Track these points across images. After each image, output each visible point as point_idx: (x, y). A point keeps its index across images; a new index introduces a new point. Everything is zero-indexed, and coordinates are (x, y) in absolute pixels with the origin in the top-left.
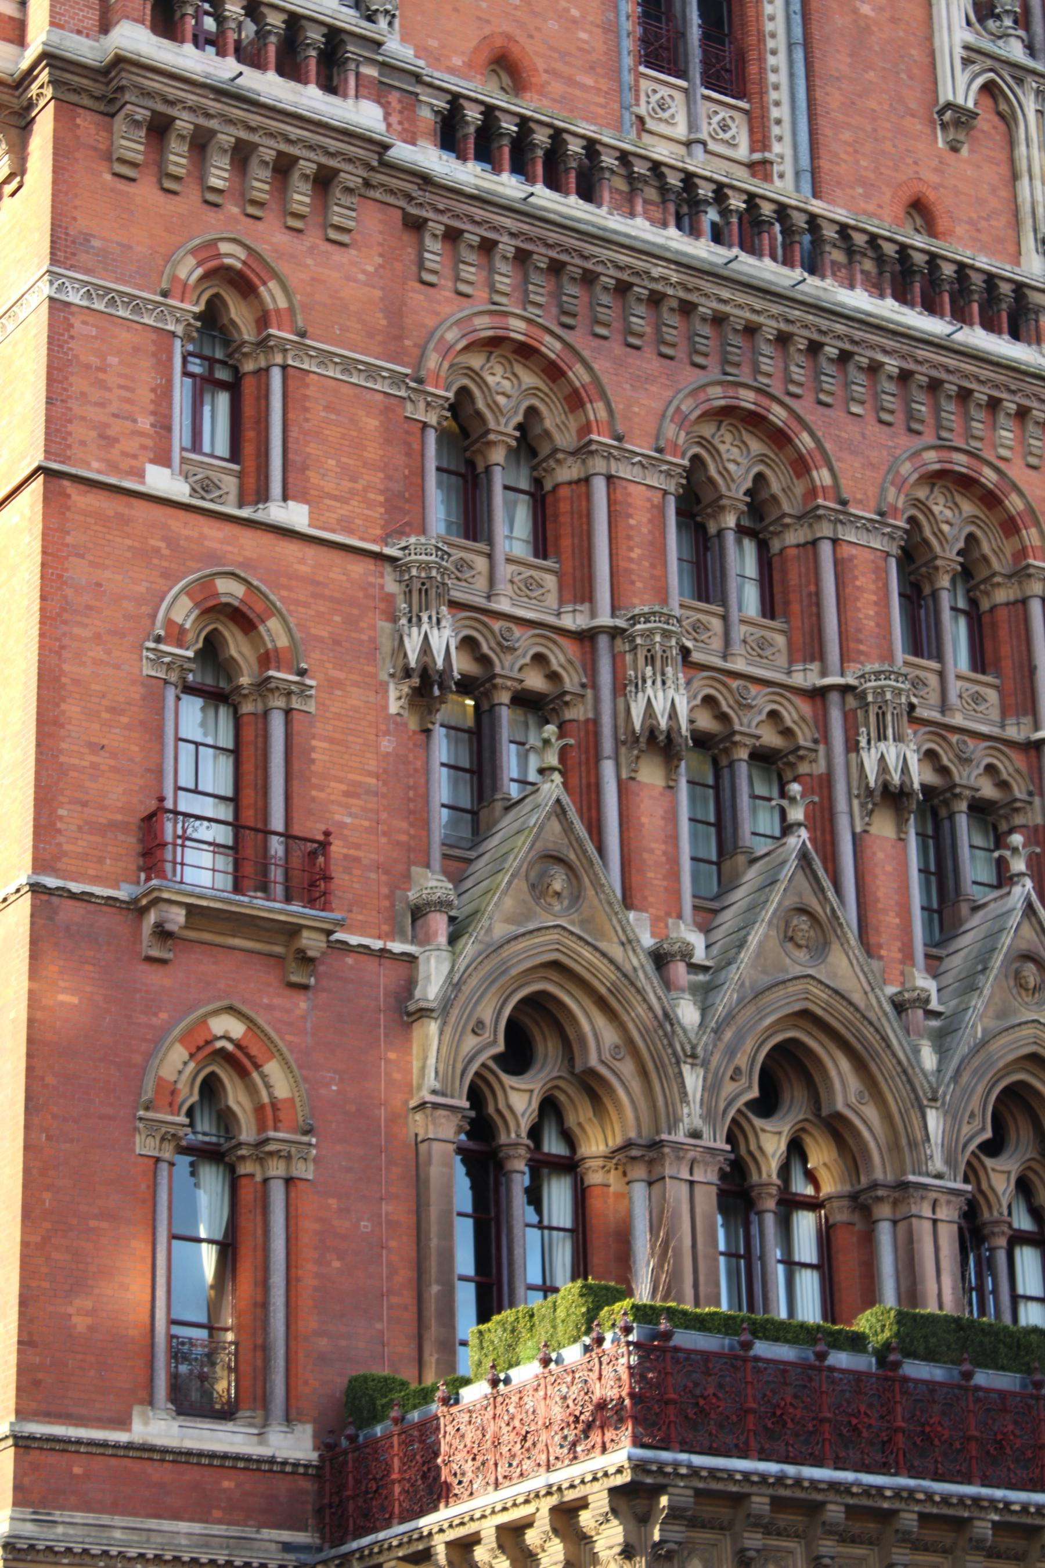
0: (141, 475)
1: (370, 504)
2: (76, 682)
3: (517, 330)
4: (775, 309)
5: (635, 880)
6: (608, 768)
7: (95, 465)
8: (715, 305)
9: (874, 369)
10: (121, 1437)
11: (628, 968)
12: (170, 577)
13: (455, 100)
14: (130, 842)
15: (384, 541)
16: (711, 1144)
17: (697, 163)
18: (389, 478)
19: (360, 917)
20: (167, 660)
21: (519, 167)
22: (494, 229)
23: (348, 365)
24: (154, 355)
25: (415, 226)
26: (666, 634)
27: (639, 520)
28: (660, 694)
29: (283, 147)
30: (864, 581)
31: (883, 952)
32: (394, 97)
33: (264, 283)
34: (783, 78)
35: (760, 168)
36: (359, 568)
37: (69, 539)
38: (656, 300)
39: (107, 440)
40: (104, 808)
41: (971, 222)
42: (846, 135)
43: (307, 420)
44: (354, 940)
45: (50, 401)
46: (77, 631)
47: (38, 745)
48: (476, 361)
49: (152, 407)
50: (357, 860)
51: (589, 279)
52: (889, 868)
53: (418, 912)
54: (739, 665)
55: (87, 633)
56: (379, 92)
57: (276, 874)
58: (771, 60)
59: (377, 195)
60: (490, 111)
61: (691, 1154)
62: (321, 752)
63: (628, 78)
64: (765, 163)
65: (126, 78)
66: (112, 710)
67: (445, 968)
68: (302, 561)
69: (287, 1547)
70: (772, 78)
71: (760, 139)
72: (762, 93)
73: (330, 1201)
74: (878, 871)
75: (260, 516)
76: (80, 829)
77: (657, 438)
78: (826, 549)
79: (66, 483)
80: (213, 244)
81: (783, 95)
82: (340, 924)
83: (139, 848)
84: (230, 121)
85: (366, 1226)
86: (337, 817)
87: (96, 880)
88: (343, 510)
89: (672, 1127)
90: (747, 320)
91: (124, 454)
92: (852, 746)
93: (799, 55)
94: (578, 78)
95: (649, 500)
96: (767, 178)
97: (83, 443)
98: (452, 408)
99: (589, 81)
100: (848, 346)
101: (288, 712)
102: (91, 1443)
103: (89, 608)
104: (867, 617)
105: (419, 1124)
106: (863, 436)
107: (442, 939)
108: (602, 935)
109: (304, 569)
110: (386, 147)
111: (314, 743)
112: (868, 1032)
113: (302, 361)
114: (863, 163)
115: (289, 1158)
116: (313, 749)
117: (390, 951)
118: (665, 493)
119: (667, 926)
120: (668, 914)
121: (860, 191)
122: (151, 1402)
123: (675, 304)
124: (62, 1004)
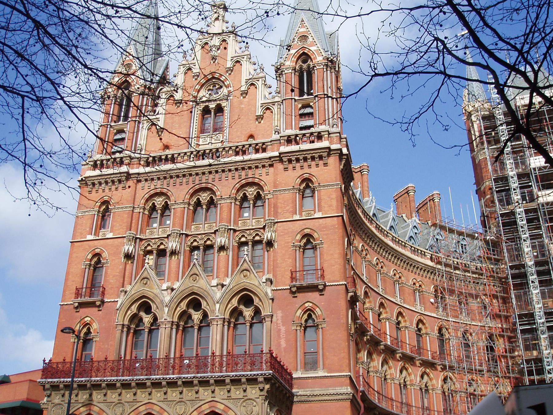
1: (123, 229)
39: (81, 234)
41: (262, 134)
42: (235, 130)
52: (223, 260)
66: (77, 275)
88: (118, 232)
104: (225, 215)
108: (152, 289)
112: (205, 293)
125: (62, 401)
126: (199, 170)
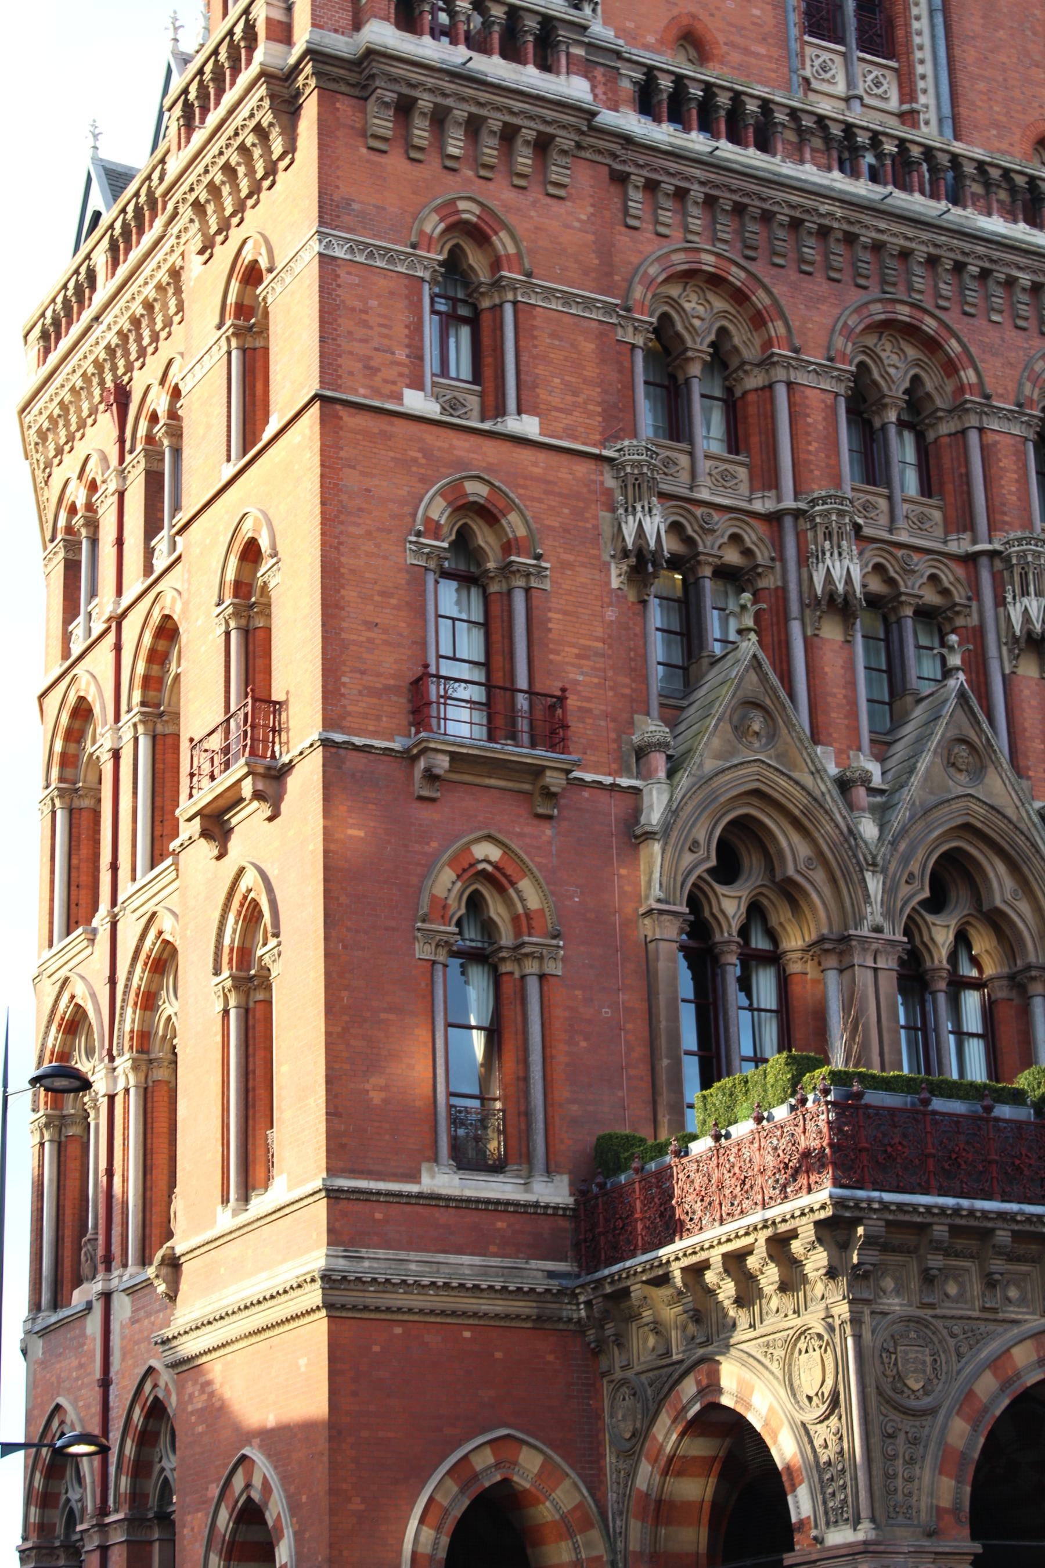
0: (399, 398)
1: (590, 415)
2: (352, 571)
3: (708, 262)
4: (925, 236)
5: (821, 719)
6: (795, 627)
7: (362, 391)
8: (874, 235)
9: (1010, 283)
10: (413, 1188)
11: (817, 793)
12: (427, 482)
13: (650, 71)
14: (402, 702)
15: (603, 445)
16: (891, 937)
17: (855, 115)
18: (604, 392)
19: (593, 758)
20: (426, 550)
21: (706, 126)
22: (686, 179)
23: (568, 299)
24: (407, 297)
25: (620, 179)
26: (841, 513)
27: (816, 418)
28: (837, 564)
29: (508, 118)
30: (1006, 462)
31: (1031, 773)
32: (599, 72)
33: (496, 233)
34: (926, 40)
35: (909, 117)
36: (582, 469)
37: (342, 454)
38: (824, 232)
39: (371, 370)
40: (379, 675)
42: (981, 86)
43: (535, 346)
44: (589, 777)
45: (322, 340)
46: (352, 529)
47: (323, 625)
48: (674, 291)
49: (407, 341)
50: (589, 711)
51: (767, 217)
52: (1034, 703)
53: (641, 753)
54: (903, 537)
55: (359, 531)
56: (585, 67)
57: (523, 725)
58: (916, 25)
59: (587, 155)
60: (679, 80)
61: (874, 946)
62: (556, 623)
63: (795, 46)
64: (913, 112)
65: (376, 68)
66: (383, 594)
67: (665, 798)
68: (535, 464)
69: (551, 1275)
70: (917, 40)
71: (908, 93)
72: (909, 53)
73: (577, 992)
74: (1025, 705)
75: (499, 428)
76: (360, 693)
77: (829, 349)
78: (973, 437)
79: (338, 407)
80: (452, 202)
81: (927, 54)
82: (577, 764)
83: (409, 707)
84: (463, 99)
85: (606, 1012)
86: (572, 676)
87: (374, 735)
88: (566, 420)
89: (858, 923)
90: (902, 247)
91: (386, 381)
92: (1000, 602)
93: (939, 19)
94: (753, 48)
95: (823, 401)
96: (915, 125)
97: (351, 373)
98: (656, 331)
99: (762, 50)
100: (987, 265)
101: (528, 590)
102: (389, 1194)
103: (360, 510)
104: (1010, 493)
105: (648, 928)
106: (1003, 339)
107: (662, 774)
108: (794, 767)
109: (537, 471)
110: (594, 114)
111: (550, 615)
112: (1020, 840)
113: (530, 298)
114: (996, 109)
115: (541, 958)
116: (549, 620)
117: (619, 786)
118: (837, 395)
119: (848, 757)
120: (850, 748)
121: (994, 132)
122: (435, 1159)
123: (840, 235)
124: (351, 837)
125: (924, 1306)
126: (896, 236)
